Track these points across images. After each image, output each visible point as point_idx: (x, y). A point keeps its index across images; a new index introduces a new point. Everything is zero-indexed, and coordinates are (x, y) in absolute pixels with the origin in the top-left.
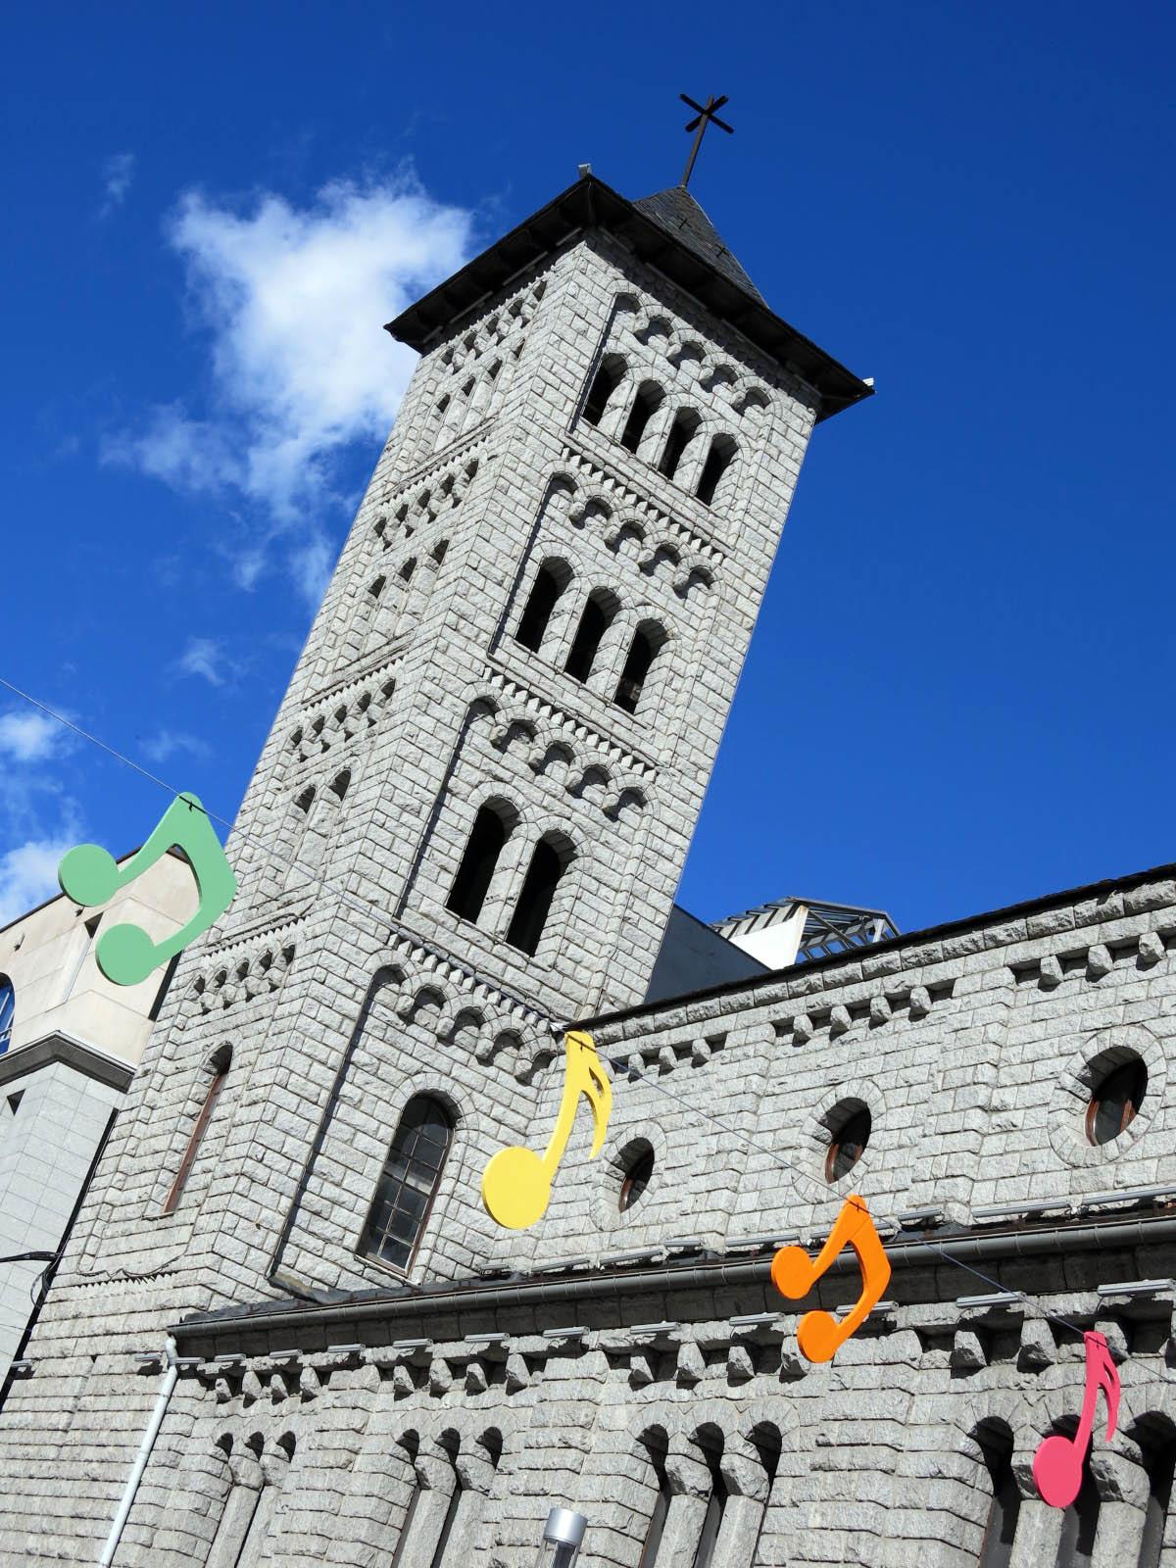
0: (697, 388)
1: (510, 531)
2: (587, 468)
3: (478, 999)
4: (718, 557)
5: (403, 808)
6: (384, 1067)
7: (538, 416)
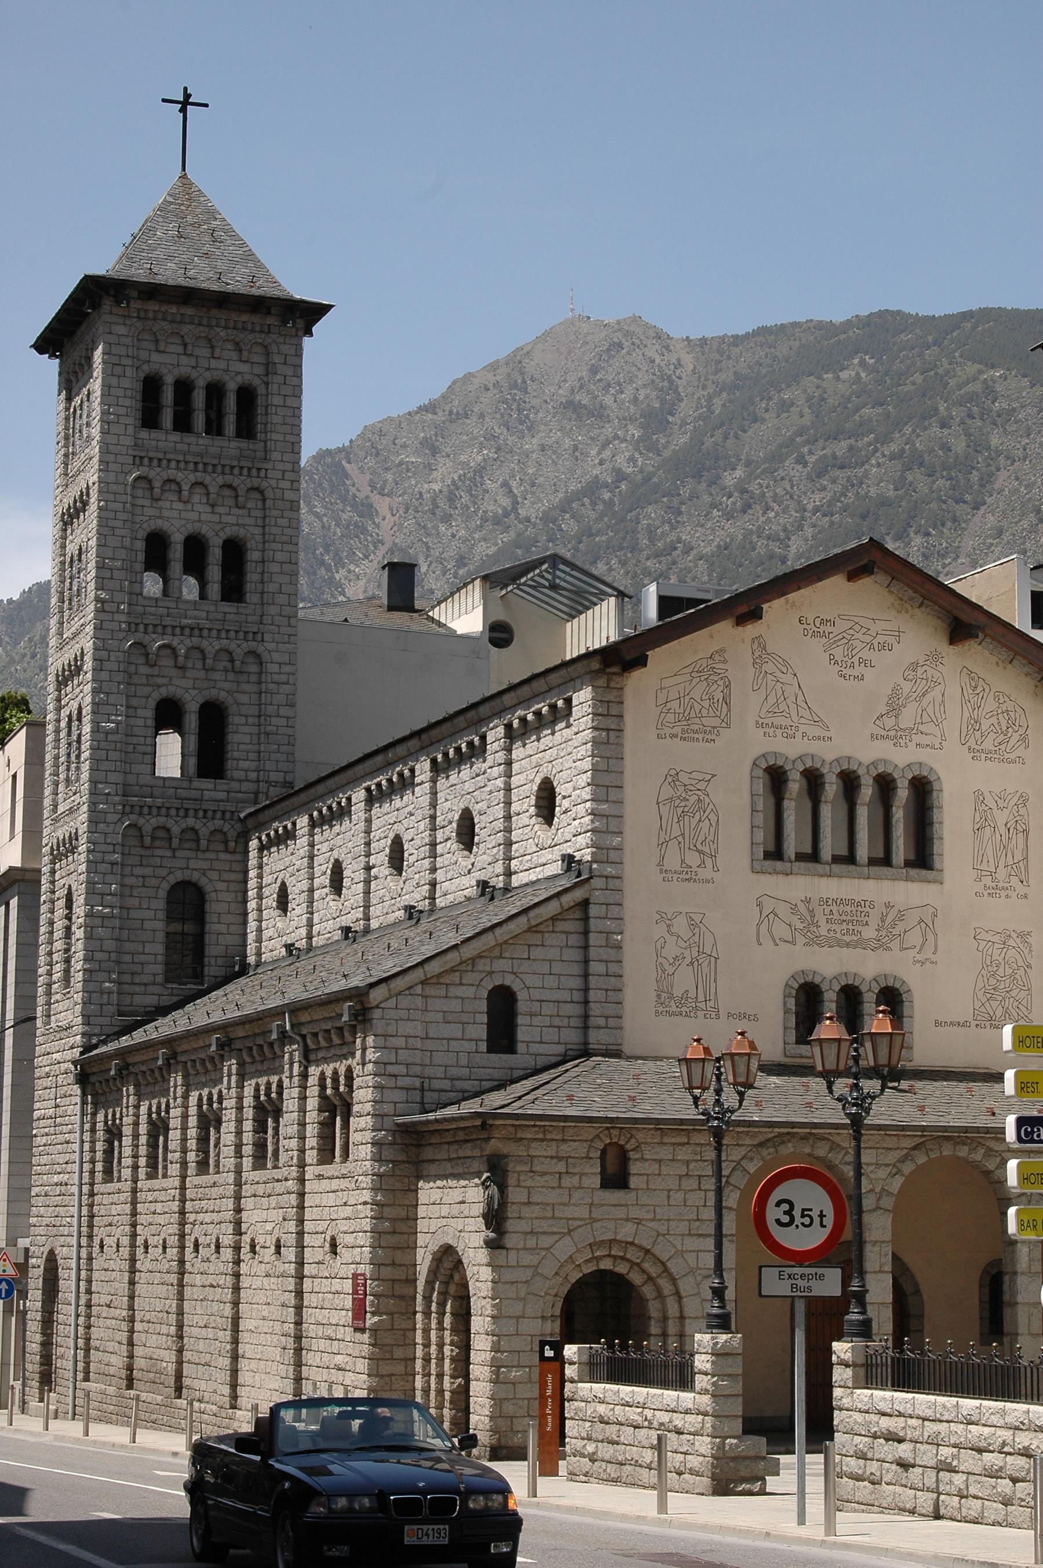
4: (262, 473)
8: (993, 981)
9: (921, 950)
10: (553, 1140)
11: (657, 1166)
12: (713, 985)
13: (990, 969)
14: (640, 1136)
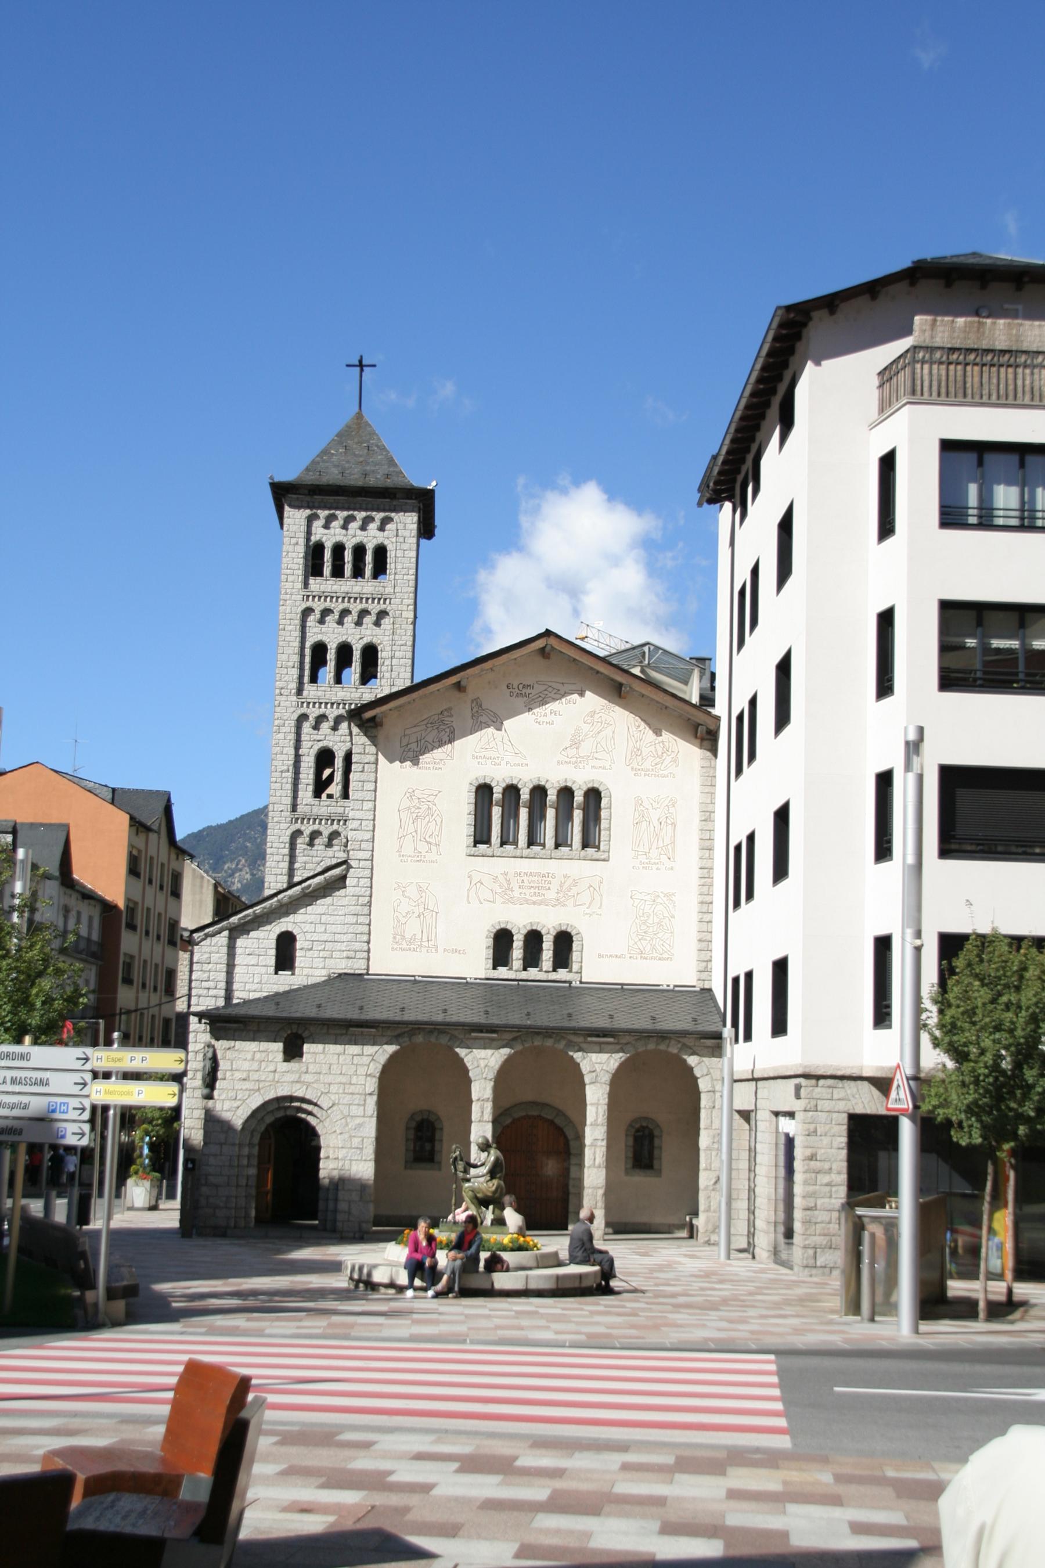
0: (359, 532)
1: (291, 644)
2: (317, 598)
3: (335, 827)
4: (388, 601)
5: (282, 772)
6: (307, 866)
7: (288, 591)
8: (644, 927)
9: (589, 906)
12: (434, 930)
13: (642, 918)
14: (312, 1029)
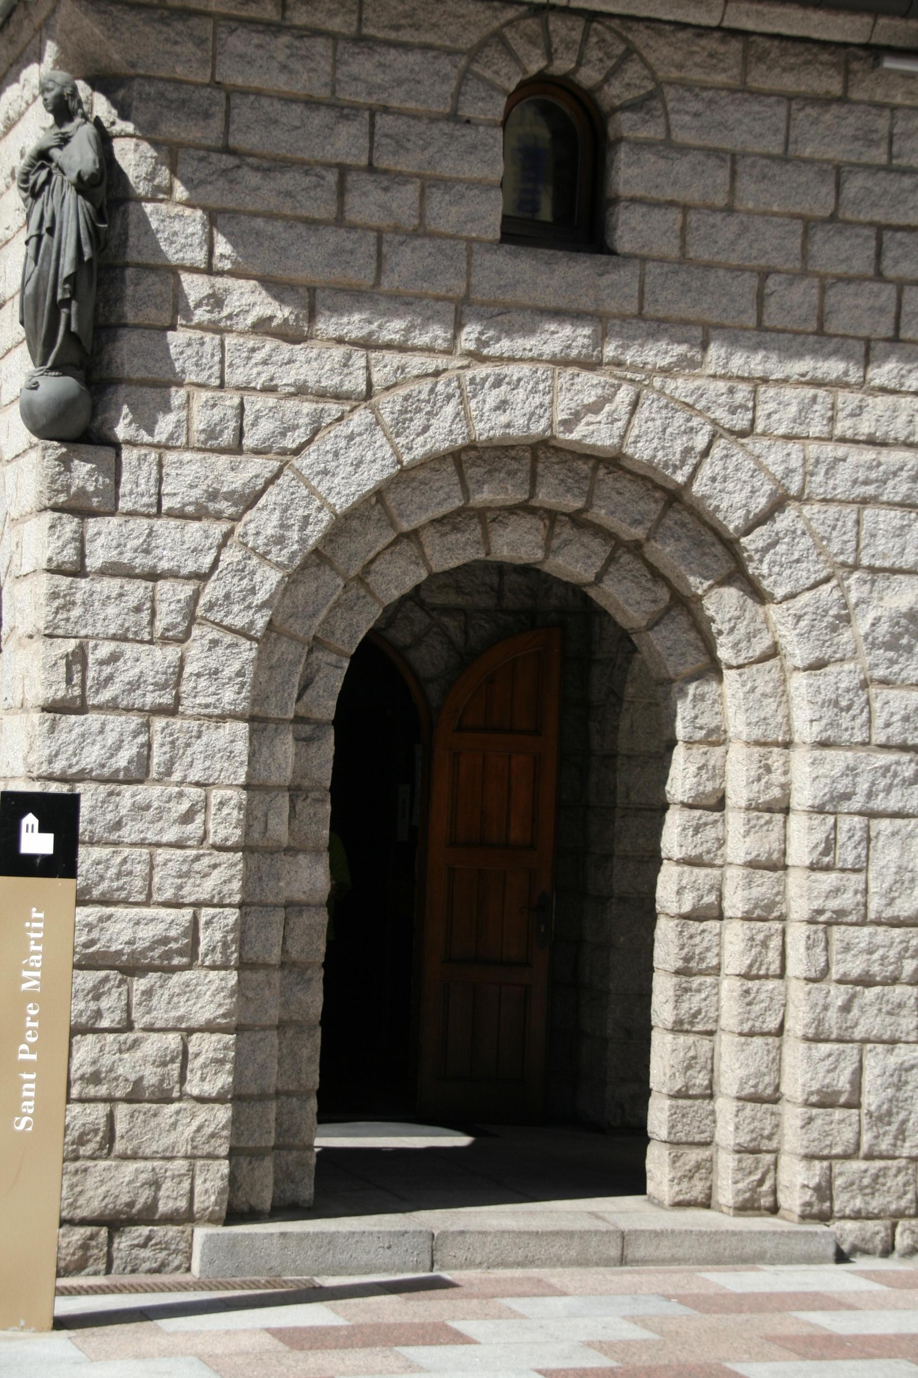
10: (316, 33)
11: (723, 176)
